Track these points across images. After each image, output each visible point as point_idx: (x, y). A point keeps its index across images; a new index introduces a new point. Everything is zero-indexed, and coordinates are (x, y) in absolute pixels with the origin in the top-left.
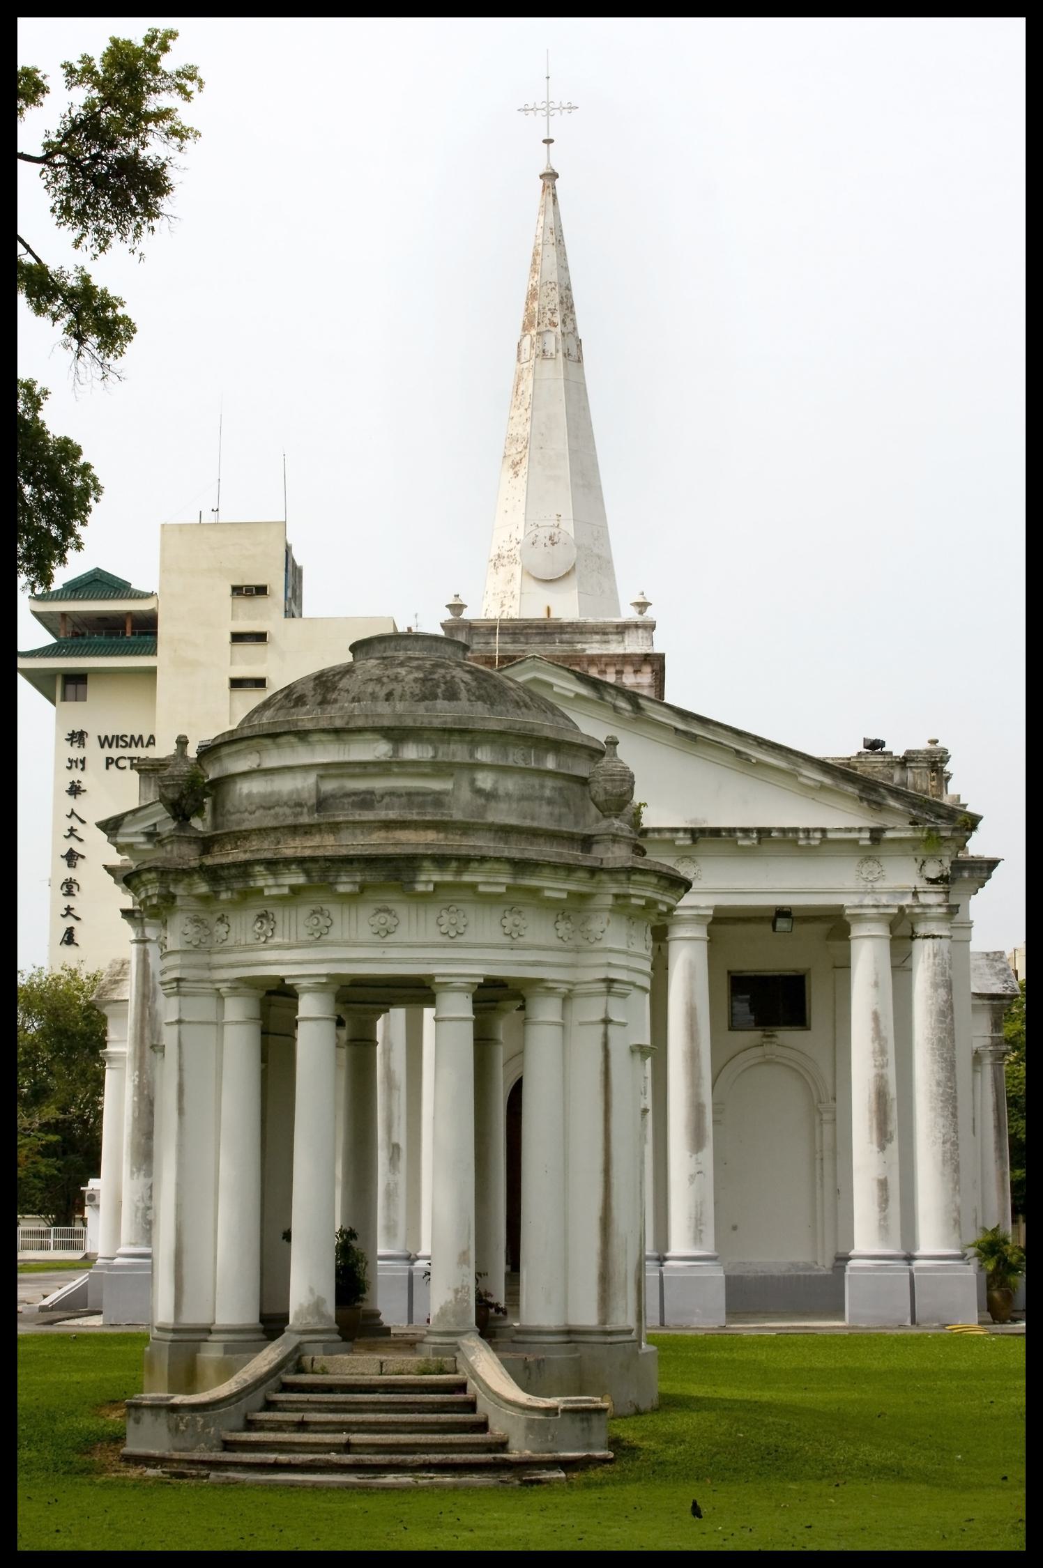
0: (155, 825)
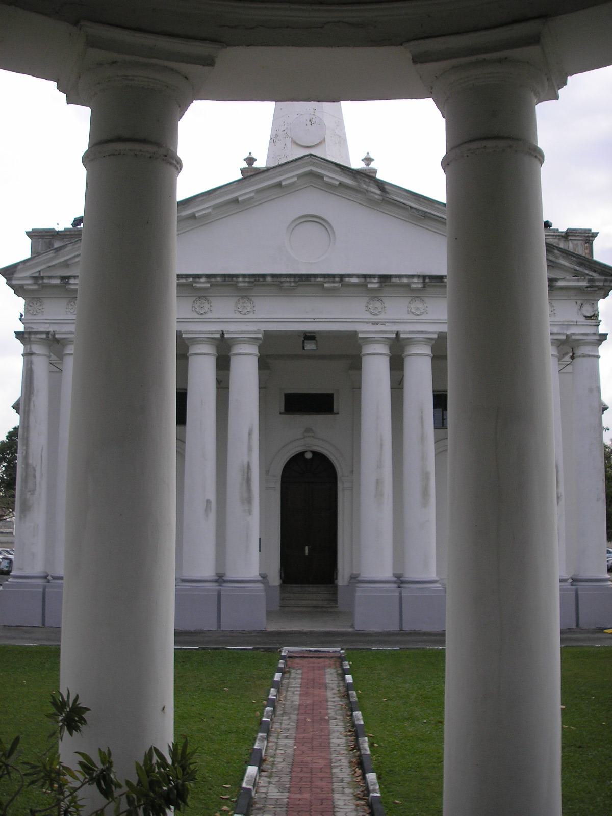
0: (39, 272)
